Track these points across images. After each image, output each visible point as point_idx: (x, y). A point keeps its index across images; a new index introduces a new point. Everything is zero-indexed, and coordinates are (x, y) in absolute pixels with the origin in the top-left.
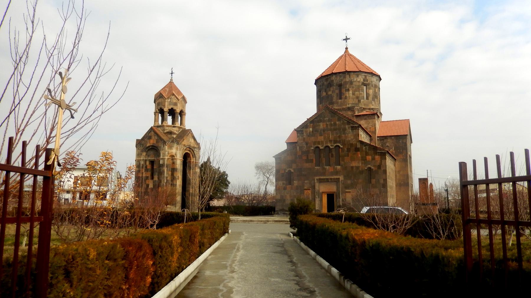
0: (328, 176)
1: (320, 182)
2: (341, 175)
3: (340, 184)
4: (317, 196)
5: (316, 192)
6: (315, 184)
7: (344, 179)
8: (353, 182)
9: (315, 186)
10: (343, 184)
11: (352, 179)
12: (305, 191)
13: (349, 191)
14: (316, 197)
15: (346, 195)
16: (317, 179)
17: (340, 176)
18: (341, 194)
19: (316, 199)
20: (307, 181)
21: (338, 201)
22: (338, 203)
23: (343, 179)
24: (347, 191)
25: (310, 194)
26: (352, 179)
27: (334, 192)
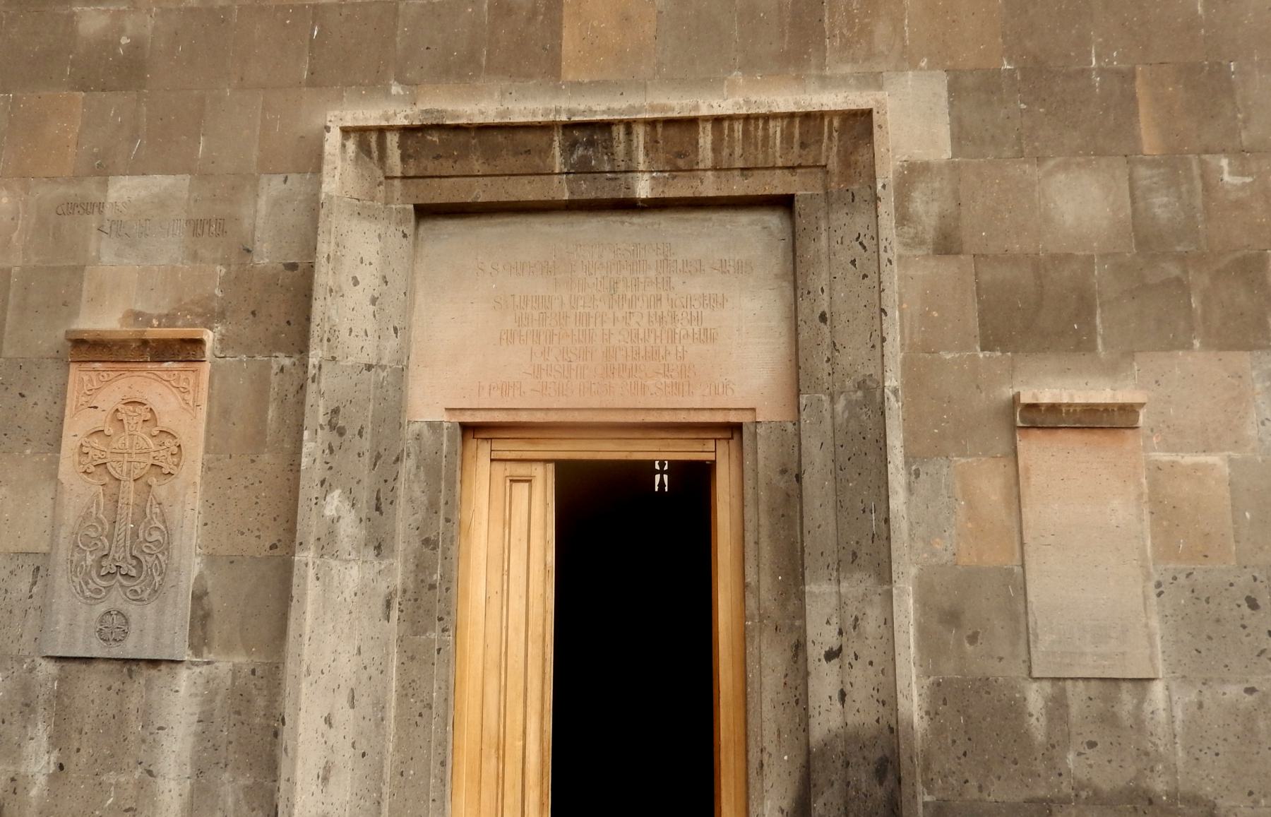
0: (599, 86)
1: (425, 212)
2: (908, 60)
3: (870, 242)
4: (334, 503)
5: (317, 411)
6: (311, 248)
7: (959, 138)
8: (1162, 205)
9: (323, 277)
10: (946, 244)
11: (1149, 140)
12: (80, 377)
13: (1102, 393)
14: (309, 524)
15: (1015, 497)
16: (359, 133)
17: (873, 81)
18: (909, 459)
19: (306, 557)
20: (161, 182)
21: (821, 635)
22: (824, 680)
23: (943, 131)
24: (1046, 396)
25: (196, 454)
26: (1149, 140)
27: (734, 429)
